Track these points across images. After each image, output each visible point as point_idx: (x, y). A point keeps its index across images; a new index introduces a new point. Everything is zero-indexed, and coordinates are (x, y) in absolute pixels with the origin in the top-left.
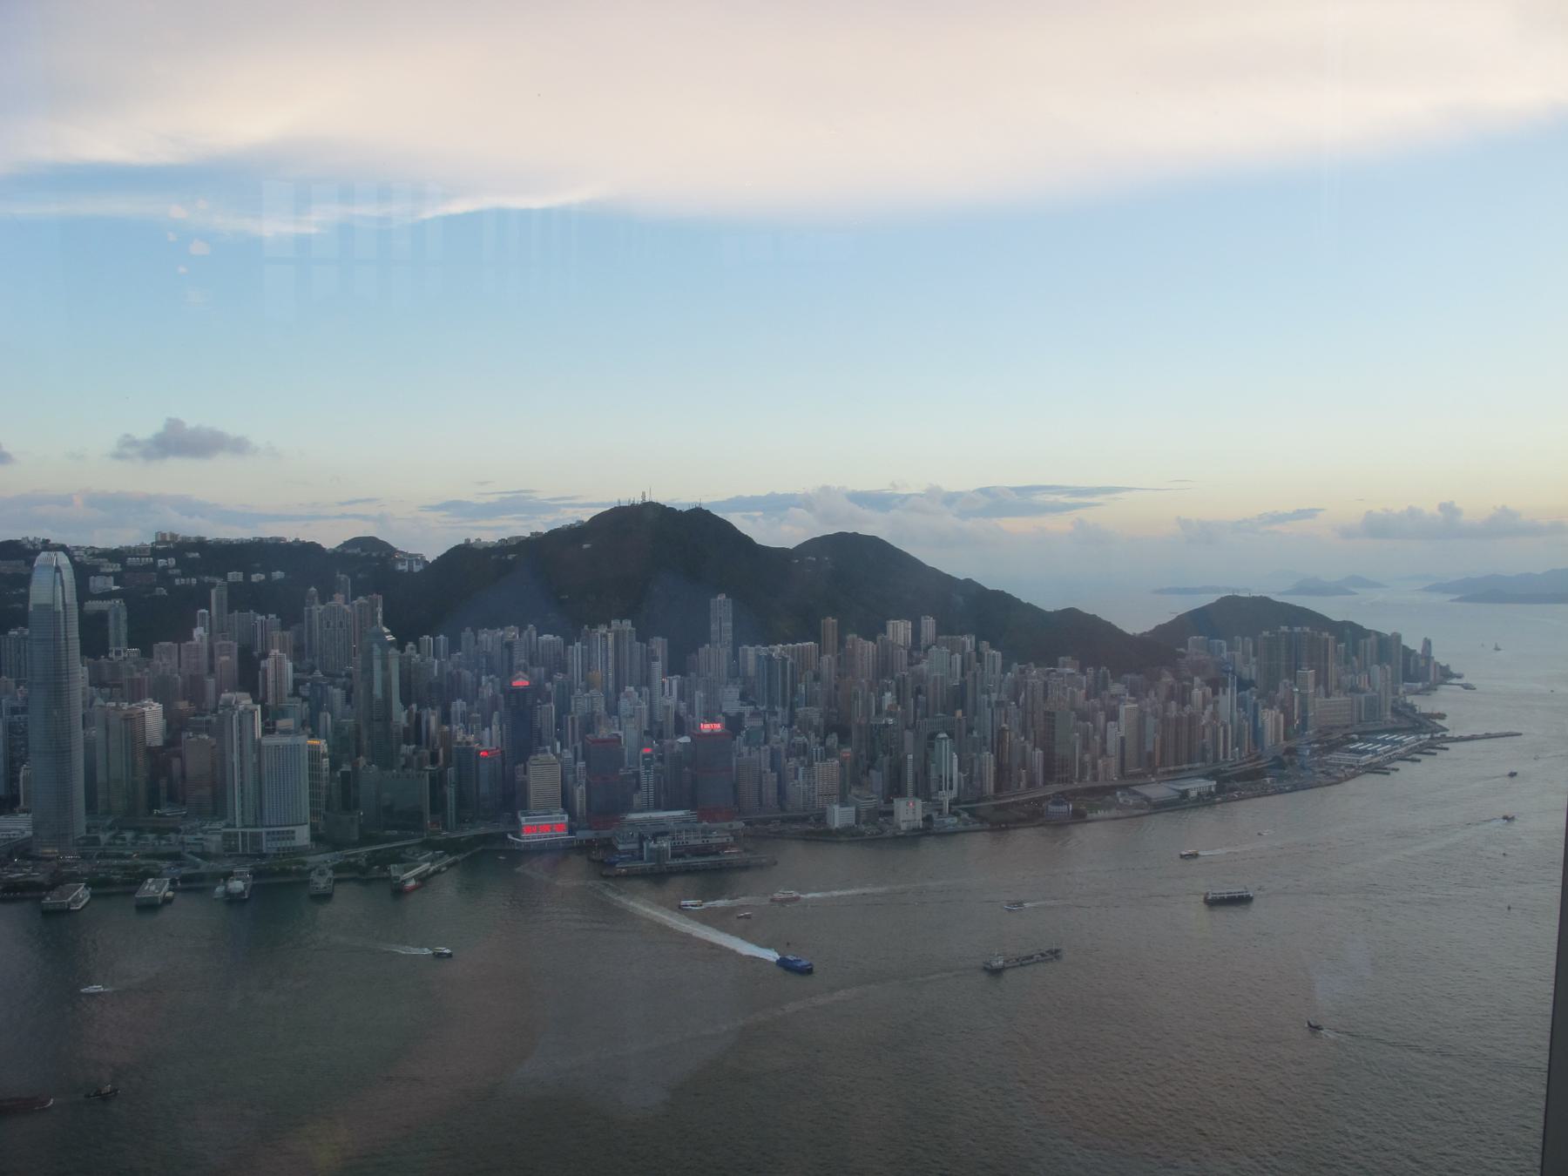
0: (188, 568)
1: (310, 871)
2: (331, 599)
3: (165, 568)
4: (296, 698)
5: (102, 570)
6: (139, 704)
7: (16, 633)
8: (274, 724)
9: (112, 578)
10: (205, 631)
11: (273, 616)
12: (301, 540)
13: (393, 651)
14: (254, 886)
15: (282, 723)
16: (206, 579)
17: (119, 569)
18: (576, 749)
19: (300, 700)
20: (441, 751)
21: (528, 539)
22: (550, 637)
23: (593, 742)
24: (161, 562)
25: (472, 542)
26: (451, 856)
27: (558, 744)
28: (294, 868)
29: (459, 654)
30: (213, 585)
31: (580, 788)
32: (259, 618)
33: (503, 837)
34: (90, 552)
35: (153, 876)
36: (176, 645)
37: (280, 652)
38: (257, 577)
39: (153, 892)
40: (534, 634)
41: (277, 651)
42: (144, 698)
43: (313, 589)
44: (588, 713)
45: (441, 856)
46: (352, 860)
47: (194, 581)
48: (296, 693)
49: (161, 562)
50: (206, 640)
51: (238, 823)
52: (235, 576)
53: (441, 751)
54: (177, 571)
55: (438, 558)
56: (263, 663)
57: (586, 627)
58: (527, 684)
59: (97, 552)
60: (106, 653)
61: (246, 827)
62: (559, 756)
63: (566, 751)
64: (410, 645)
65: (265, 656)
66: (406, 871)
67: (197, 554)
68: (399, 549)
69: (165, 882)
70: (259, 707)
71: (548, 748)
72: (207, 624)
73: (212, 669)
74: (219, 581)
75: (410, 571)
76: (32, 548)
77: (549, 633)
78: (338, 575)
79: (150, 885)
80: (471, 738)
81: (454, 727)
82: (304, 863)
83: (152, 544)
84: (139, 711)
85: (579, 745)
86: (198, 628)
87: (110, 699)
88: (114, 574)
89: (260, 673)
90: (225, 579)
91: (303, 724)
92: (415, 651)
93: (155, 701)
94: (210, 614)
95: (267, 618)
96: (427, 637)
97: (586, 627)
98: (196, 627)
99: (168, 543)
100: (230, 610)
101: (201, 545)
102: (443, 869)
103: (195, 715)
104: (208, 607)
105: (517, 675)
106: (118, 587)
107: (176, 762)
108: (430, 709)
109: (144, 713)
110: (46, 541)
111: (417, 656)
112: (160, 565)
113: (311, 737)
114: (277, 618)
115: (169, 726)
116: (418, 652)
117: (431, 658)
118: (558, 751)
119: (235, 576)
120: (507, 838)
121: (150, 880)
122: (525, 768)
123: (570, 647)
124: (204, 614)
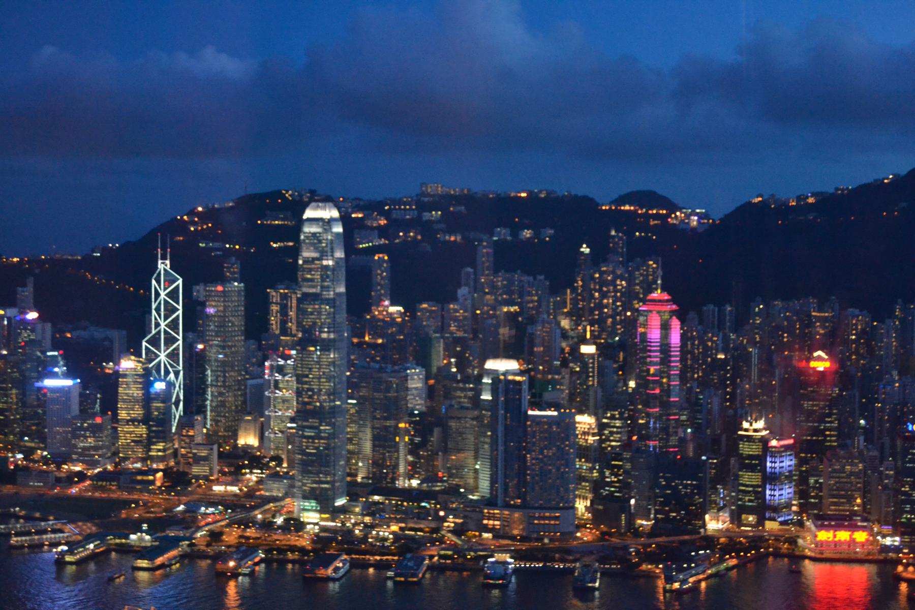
0: (452, 223)
1: (575, 561)
2: (605, 261)
3: (430, 222)
4: (563, 370)
5: (369, 223)
6: (400, 366)
7: (282, 286)
8: (541, 396)
9: (376, 232)
10: (469, 292)
11: (542, 277)
12: (573, 193)
13: (676, 324)
14: (516, 571)
15: (548, 396)
16: (472, 235)
17: (383, 222)
18: (883, 444)
19: (568, 370)
20: (724, 437)
21: (832, 194)
22: (857, 312)
23: (906, 439)
24: (426, 216)
25: (766, 197)
26: (731, 557)
27: (862, 438)
28: (557, 555)
29: (747, 327)
30: (481, 241)
31: (886, 492)
32: (525, 278)
33: (793, 541)
34: (355, 203)
35: (410, 550)
36: (440, 305)
37: (548, 316)
38: (527, 234)
39: (411, 568)
40: (837, 306)
41: (545, 316)
42: (405, 360)
43: (585, 249)
44: (899, 404)
45: (722, 560)
46: (620, 553)
47: (459, 238)
48: (565, 363)
49: (426, 216)
50: (469, 302)
51: (500, 502)
52: (502, 233)
53: (724, 437)
54: (442, 226)
55: (726, 216)
56: (530, 330)
57: (900, 301)
58: (828, 364)
59: (362, 203)
60: (369, 311)
61: (507, 506)
62: (861, 453)
63: (870, 446)
64: (692, 315)
65: (532, 320)
66: (680, 570)
67: (463, 208)
68: (681, 205)
69: (424, 559)
70: (527, 375)
71: (849, 442)
72: (472, 283)
73: (475, 332)
74: (485, 237)
75: (694, 229)
76: (298, 199)
77: (856, 308)
78: (613, 233)
79: (410, 560)
80: (760, 424)
81: (739, 411)
82: (568, 551)
83: (417, 195)
84: (404, 374)
85: (887, 440)
86: (463, 288)
87: (373, 359)
88: (379, 227)
89: (526, 339)
90: (492, 235)
91: (572, 396)
92: (697, 323)
93: (418, 364)
94: (475, 273)
95: (535, 279)
96: (711, 307)
97: (900, 301)
98: (460, 287)
99: (433, 196)
100: (496, 272)
101: (467, 199)
102: (724, 572)
103: (458, 382)
104: (474, 266)
105: (816, 354)
106: (383, 241)
107: (437, 431)
108: (712, 389)
109: (407, 375)
110: (313, 193)
111: (699, 327)
112: (424, 219)
113: (581, 412)
114: (545, 279)
115: (431, 393)
116: (700, 324)
117: (716, 330)
118: (862, 447)
119: (502, 233)
120: (795, 542)
121: (409, 556)
122: (822, 461)
123: (880, 324)
124: (468, 274)
